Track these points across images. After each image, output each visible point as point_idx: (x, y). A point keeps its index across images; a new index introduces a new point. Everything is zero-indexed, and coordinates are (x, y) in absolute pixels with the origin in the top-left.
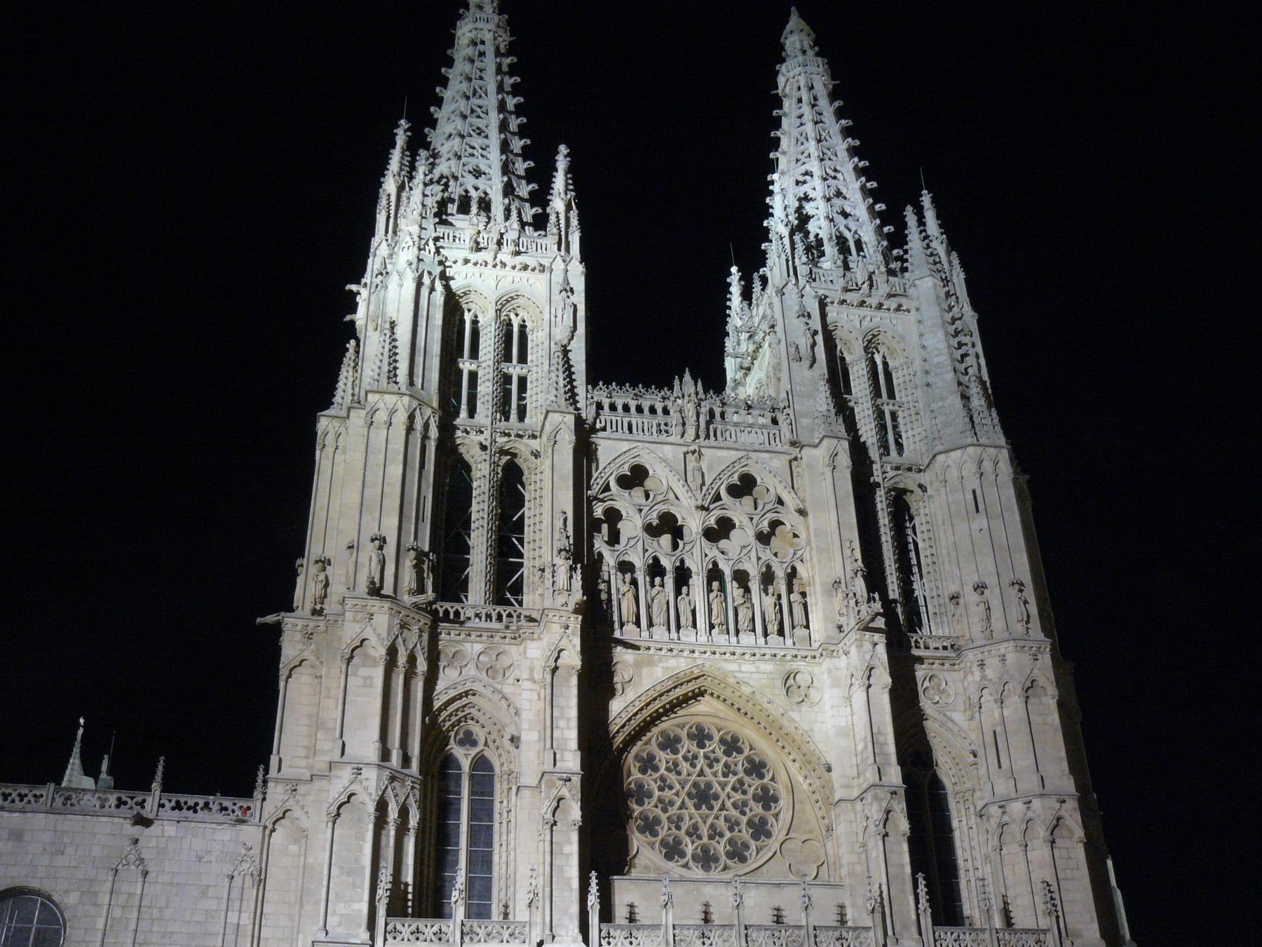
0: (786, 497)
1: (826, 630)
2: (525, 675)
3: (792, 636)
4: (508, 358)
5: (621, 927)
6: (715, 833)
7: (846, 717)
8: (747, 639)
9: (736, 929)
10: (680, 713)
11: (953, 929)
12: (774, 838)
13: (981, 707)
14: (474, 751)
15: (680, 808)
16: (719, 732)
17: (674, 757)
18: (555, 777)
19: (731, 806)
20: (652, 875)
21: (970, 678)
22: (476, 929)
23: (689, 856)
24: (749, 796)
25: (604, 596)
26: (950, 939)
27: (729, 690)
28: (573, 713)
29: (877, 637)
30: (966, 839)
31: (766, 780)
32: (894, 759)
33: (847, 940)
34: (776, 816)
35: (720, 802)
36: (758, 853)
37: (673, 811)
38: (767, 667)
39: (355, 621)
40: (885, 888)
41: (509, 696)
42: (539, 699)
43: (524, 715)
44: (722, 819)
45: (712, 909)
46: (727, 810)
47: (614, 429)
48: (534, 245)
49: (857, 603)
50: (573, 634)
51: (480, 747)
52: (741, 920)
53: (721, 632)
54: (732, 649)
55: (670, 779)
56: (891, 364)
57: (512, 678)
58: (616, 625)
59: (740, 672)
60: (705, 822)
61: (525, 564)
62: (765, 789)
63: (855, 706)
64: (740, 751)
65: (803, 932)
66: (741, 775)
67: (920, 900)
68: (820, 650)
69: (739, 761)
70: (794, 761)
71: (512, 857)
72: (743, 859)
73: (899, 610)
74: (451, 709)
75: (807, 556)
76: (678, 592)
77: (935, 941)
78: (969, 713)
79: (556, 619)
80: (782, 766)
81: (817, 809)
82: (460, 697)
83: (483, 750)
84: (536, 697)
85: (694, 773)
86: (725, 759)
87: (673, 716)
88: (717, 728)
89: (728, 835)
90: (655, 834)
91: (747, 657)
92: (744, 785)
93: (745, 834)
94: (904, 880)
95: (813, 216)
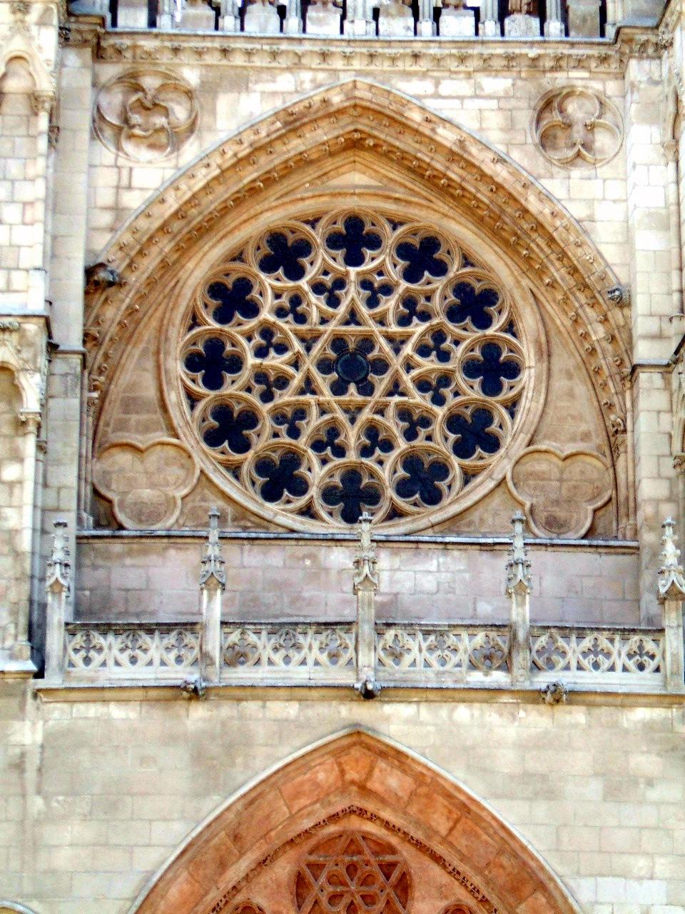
12: (502, 451)
17: (291, 284)
19: (410, 385)
23: (314, 492)
31: (490, 331)
34: (512, 407)
37: (285, 398)
38: (497, 84)
44: (391, 412)
46: (402, 394)
50: (42, 23)
55: (282, 330)
60: (353, 421)
62: (491, 348)
64: (440, 269)
66: (440, 319)
69: (438, 290)
72: (433, 497)
85: (333, 316)
86: (404, 285)
88: (390, 221)
89: (402, 445)
92: (444, 340)
93: (441, 443)
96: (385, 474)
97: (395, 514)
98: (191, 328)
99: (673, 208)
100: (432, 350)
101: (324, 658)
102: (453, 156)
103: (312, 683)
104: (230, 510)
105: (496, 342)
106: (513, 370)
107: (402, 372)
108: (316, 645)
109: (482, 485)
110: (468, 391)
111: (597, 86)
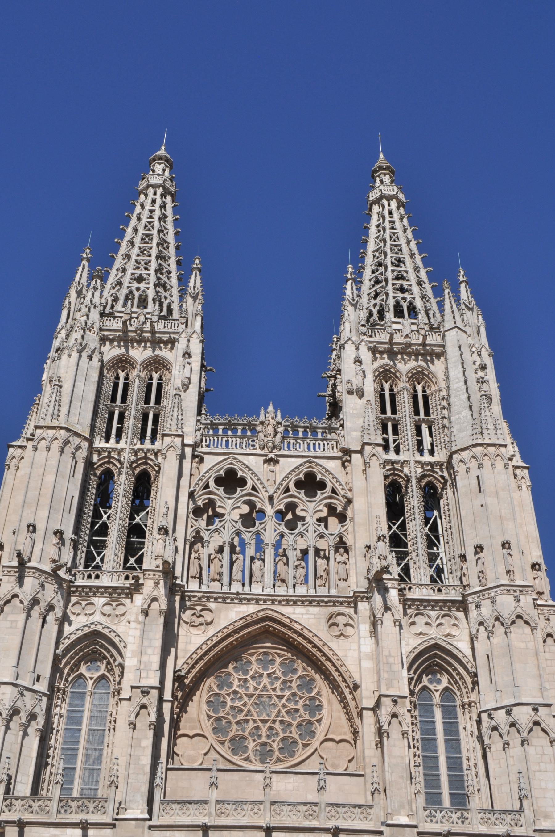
0: (339, 488)
4: (147, 401)
12: (316, 739)
18: (139, 691)
23: (250, 752)
34: (319, 721)
39: (8, 582)
43: (129, 647)
44: (278, 723)
47: (215, 446)
48: (169, 325)
55: (241, 694)
56: (428, 392)
57: (125, 621)
60: (264, 727)
61: (146, 543)
72: (292, 754)
75: (350, 529)
79: (152, 576)
95: (380, 293)
96: (275, 745)
97: (279, 760)
98: (209, 692)
101: (252, 814)
102: (300, 635)
104: (221, 759)
106: (320, 707)
108: (249, 809)
109: (310, 750)
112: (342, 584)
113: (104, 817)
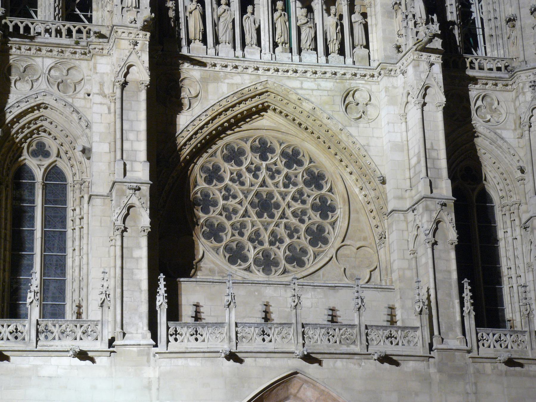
1: (385, 50)
2: (95, 89)
3: (352, 55)
5: (187, 325)
6: (275, 240)
7: (401, 133)
8: (309, 57)
9: (293, 326)
10: (245, 127)
11: (495, 330)
12: (330, 245)
13: (530, 127)
14: (46, 162)
15: (243, 216)
16: (280, 145)
17: (238, 168)
18: (125, 187)
19: (290, 215)
20: (217, 278)
21: (521, 98)
22: (51, 328)
24: (308, 206)
25: (171, 14)
26: (492, 340)
27: (291, 106)
28: (142, 126)
29: (434, 57)
30: (511, 248)
31: (324, 191)
32: (445, 173)
33: (396, 338)
34: (333, 224)
35: (281, 210)
36: (315, 258)
37: (237, 218)
38: (328, 84)
40: (432, 292)
41: (80, 110)
42: (109, 113)
43: (96, 128)
44: (282, 226)
45: (271, 309)
46: (287, 218)
49: (415, 24)
50: (142, 50)
51: (53, 158)
52: (299, 319)
53: (284, 51)
54: (294, 67)
58: (184, 43)
59: (302, 88)
60: (266, 229)
62: (323, 199)
63: (409, 123)
64: (300, 163)
65: (355, 331)
66: (301, 186)
67: (465, 303)
68: (379, 69)
70: (351, 174)
71: (85, 261)
72: (301, 264)
73: (456, 32)
74: (23, 121)
76: (243, 11)
77: (478, 341)
78: (519, 131)
79: (125, 35)
80: (340, 179)
81: (371, 219)
82: (32, 110)
83: (56, 161)
84: (107, 111)
86: (285, 171)
87: (237, 130)
88: (279, 142)
89: (287, 241)
90: (219, 240)
91: (308, 74)
93: (304, 241)
94: (451, 285)
99: (405, 142)
100: (298, 200)
103: (276, 350)
105: (325, 196)
106: (333, 209)
107: (286, 209)
110: (315, 218)
111: (368, 87)
112: (360, 52)
113: (98, 343)
